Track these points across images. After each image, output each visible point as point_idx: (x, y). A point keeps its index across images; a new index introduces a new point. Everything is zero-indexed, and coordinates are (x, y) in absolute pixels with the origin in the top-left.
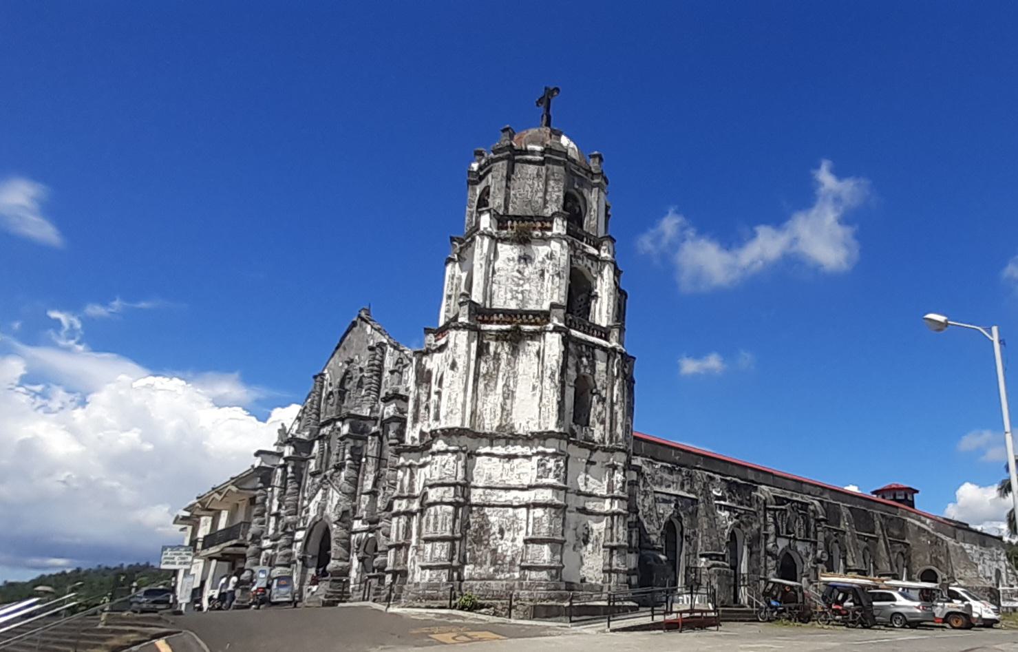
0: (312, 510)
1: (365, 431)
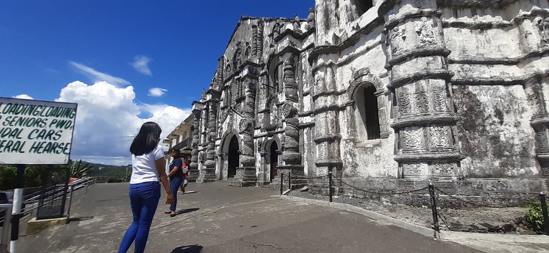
0: (224, 128)
1: (256, 73)
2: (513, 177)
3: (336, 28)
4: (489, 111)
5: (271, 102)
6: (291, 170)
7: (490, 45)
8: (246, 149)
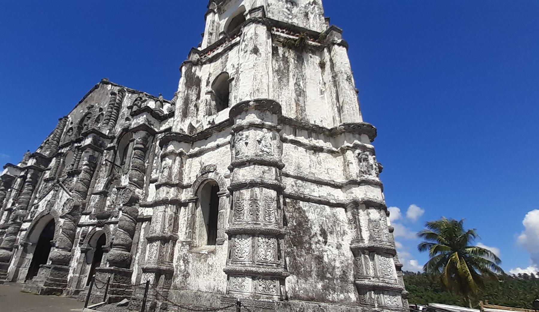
0: (40, 206)
1: (102, 145)
2: (333, 302)
3: (194, 118)
4: (315, 229)
5: (112, 183)
6: (113, 275)
7: (320, 166)
8: (61, 240)
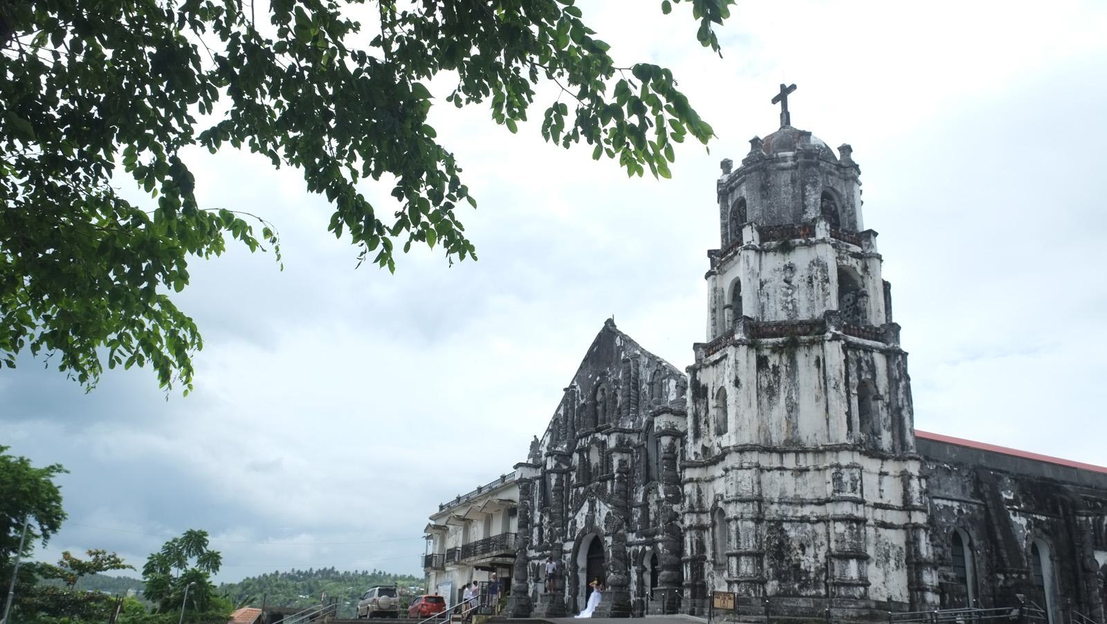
0: (578, 522)
